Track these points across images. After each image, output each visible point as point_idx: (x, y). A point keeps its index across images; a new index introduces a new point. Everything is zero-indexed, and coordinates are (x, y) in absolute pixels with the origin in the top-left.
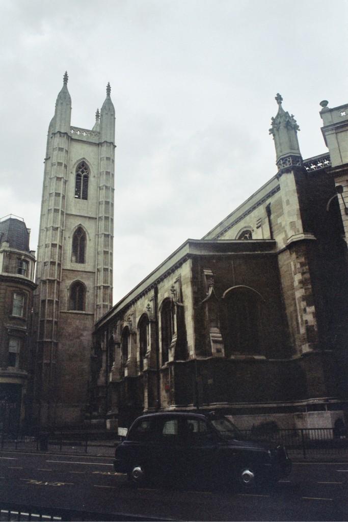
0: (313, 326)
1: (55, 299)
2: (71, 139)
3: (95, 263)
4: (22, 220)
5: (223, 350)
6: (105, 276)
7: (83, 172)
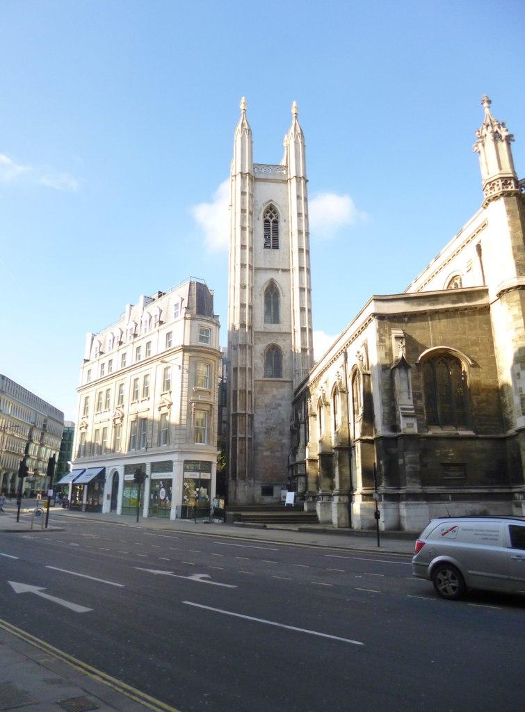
1: (248, 366)
4: (203, 283)
5: (415, 425)
7: (271, 217)
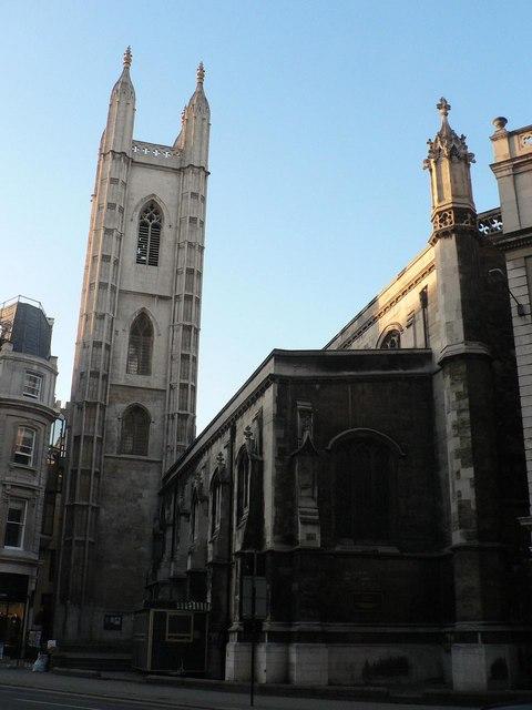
0: (469, 501)
1: (97, 435)
2: (132, 163)
3: (166, 374)
4: (37, 306)
5: (318, 537)
6: (184, 397)
7: (151, 218)
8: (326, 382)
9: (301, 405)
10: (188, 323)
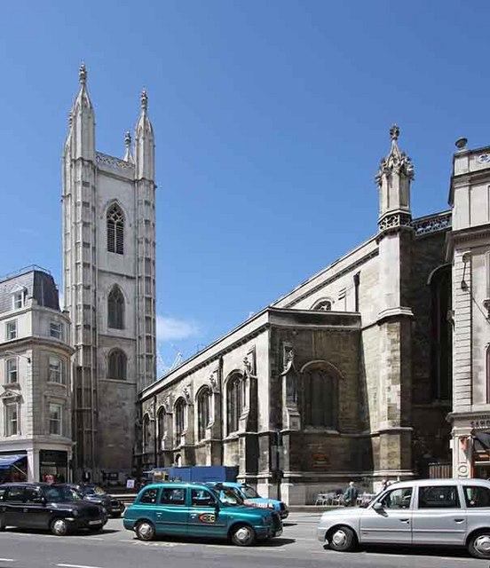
6: (149, 345)
8: (301, 331)
9: (286, 344)
10: (149, 296)
